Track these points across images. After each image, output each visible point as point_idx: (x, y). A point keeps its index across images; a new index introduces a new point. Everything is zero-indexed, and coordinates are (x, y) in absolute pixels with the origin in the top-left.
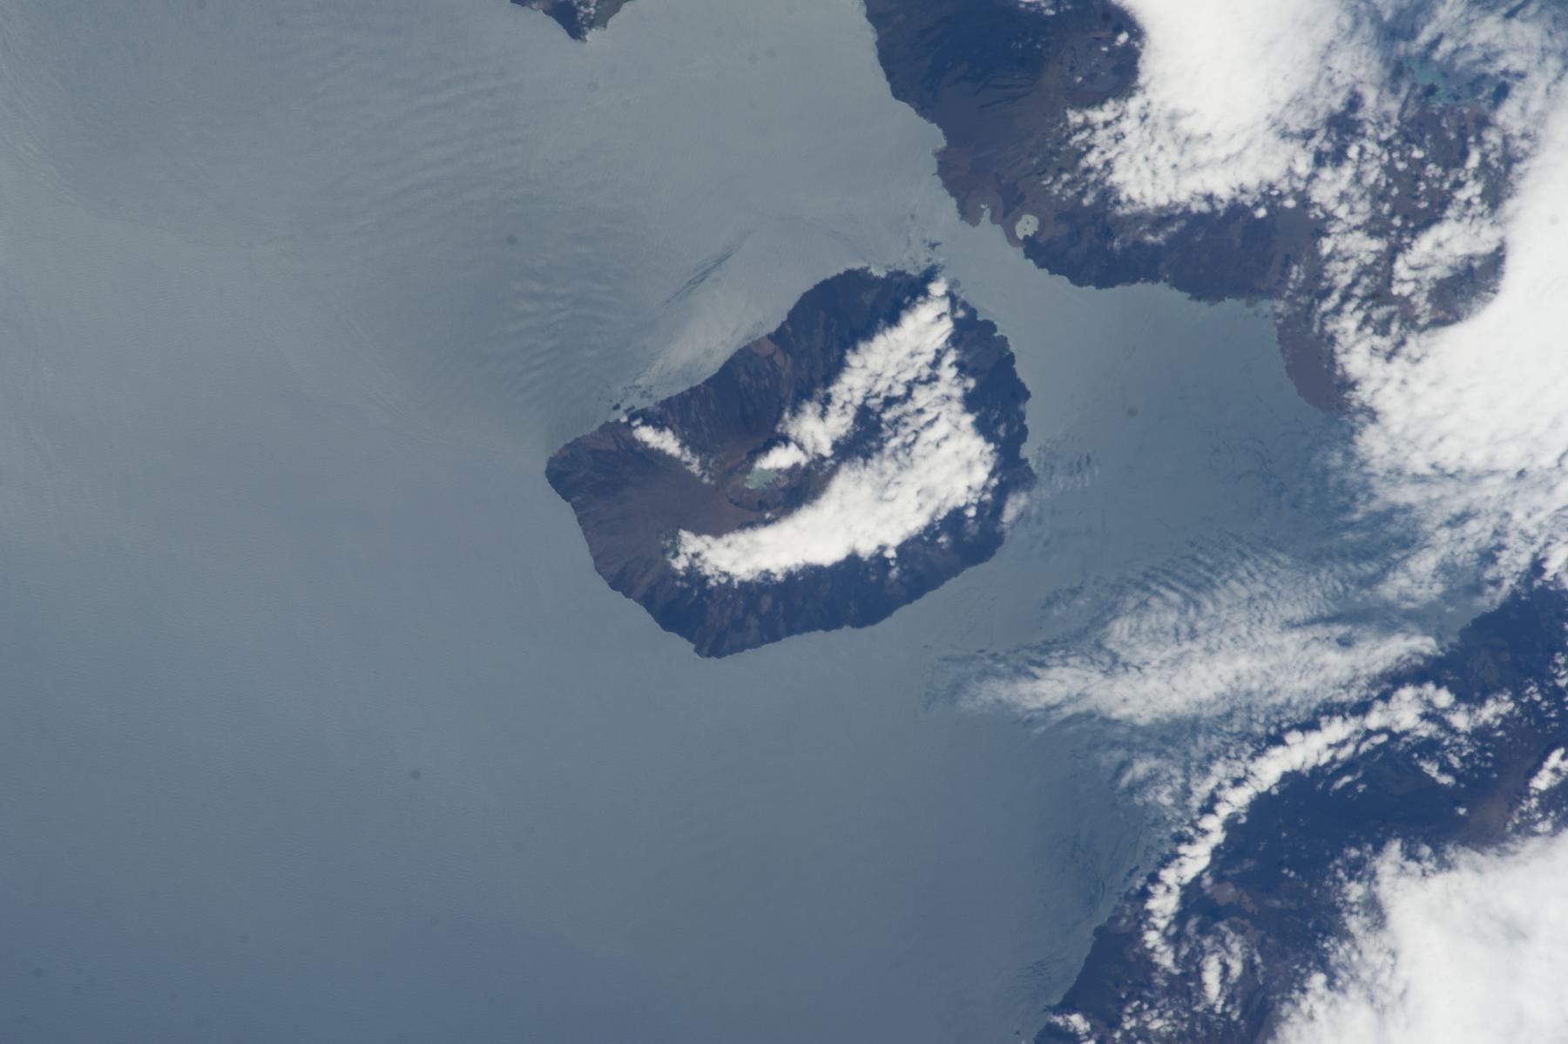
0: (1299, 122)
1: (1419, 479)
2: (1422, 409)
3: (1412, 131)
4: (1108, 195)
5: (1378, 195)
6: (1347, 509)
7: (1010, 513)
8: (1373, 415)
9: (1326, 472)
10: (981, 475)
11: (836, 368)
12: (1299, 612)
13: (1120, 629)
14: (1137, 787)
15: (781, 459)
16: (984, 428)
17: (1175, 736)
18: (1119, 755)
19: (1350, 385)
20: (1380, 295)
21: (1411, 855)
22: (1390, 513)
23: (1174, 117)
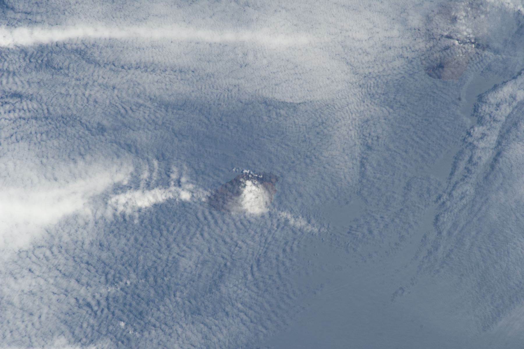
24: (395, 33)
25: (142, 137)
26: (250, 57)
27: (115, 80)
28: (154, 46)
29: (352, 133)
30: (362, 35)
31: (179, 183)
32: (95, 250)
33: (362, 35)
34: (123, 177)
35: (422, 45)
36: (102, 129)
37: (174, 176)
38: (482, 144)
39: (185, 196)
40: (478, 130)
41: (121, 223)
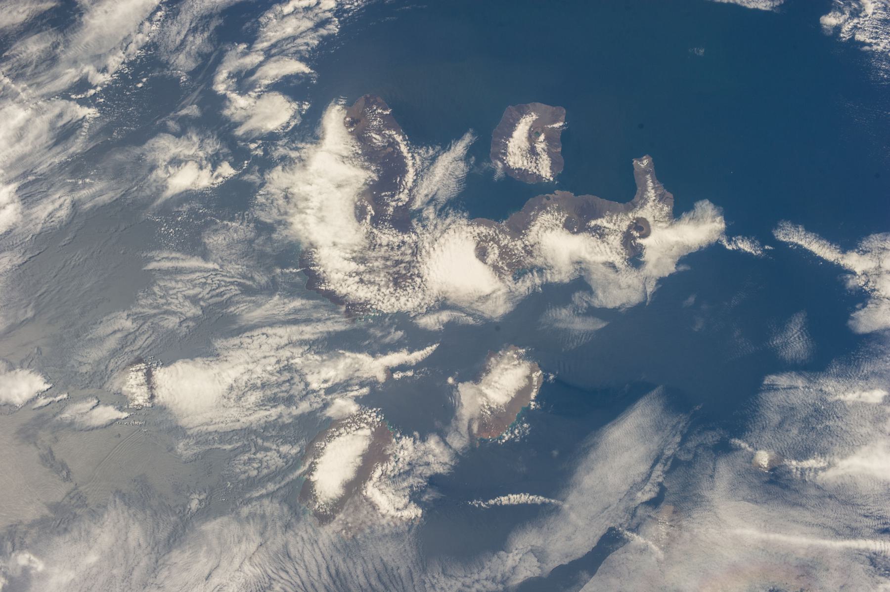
0: (537, 246)
1: (450, 224)
2: (463, 233)
3: (519, 262)
4: (547, 212)
5: (511, 250)
6: (454, 210)
7: (499, 163)
8: (468, 225)
9: (464, 211)
10: (511, 164)
11: (549, 156)
12: (440, 192)
13: (462, 165)
14: (428, 149)
15: (542, 138)
16: (520, 169)
17: (433, 160)
18: (436, 150)
19: (478, 225)
20: (493, 239)
21: (373, 181)
22: (447, 216)
23: (552, 229)
24: (696, 530)
25: (812, 491)
26: (763, 525)
27: (823, 520)
28: (804, 534)
29: (718, 484)
30: (711, 531)
31: (797, 468)
32: (834, 441)
33: (711, 531)
34: (821, 474)
35: (684, 523)
36: (830, 497)
37: (799, 472)
38: (659, 473)
39: (794, 463)
40: (660, 480)
41: (823, 453)
